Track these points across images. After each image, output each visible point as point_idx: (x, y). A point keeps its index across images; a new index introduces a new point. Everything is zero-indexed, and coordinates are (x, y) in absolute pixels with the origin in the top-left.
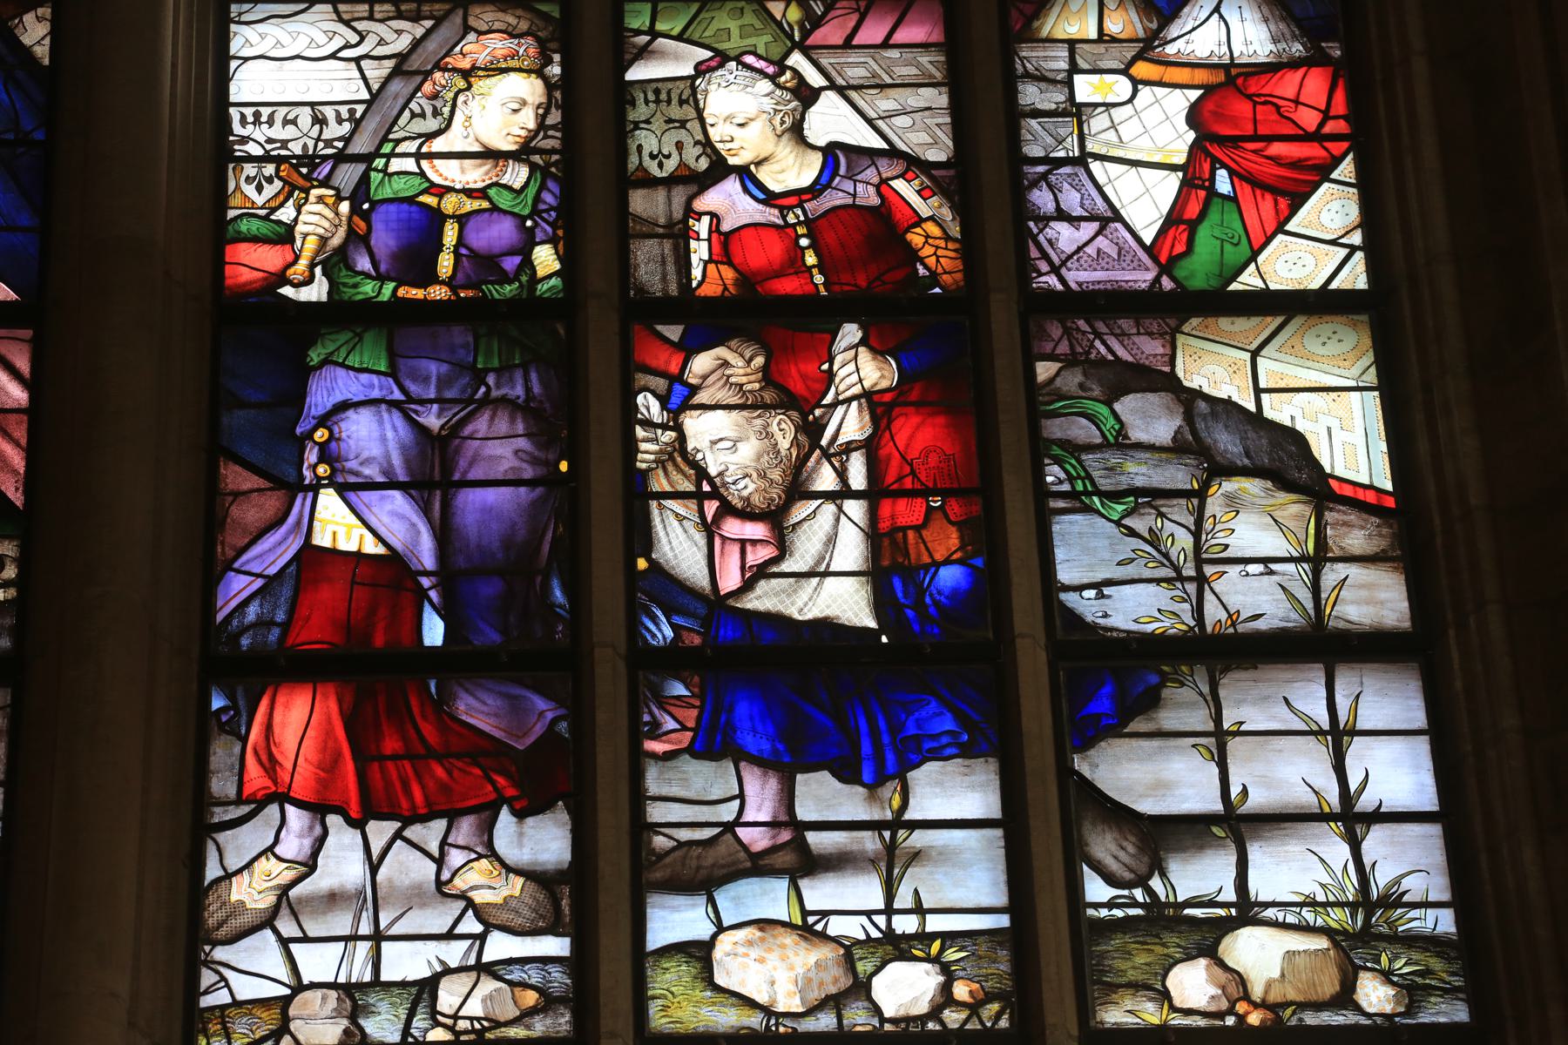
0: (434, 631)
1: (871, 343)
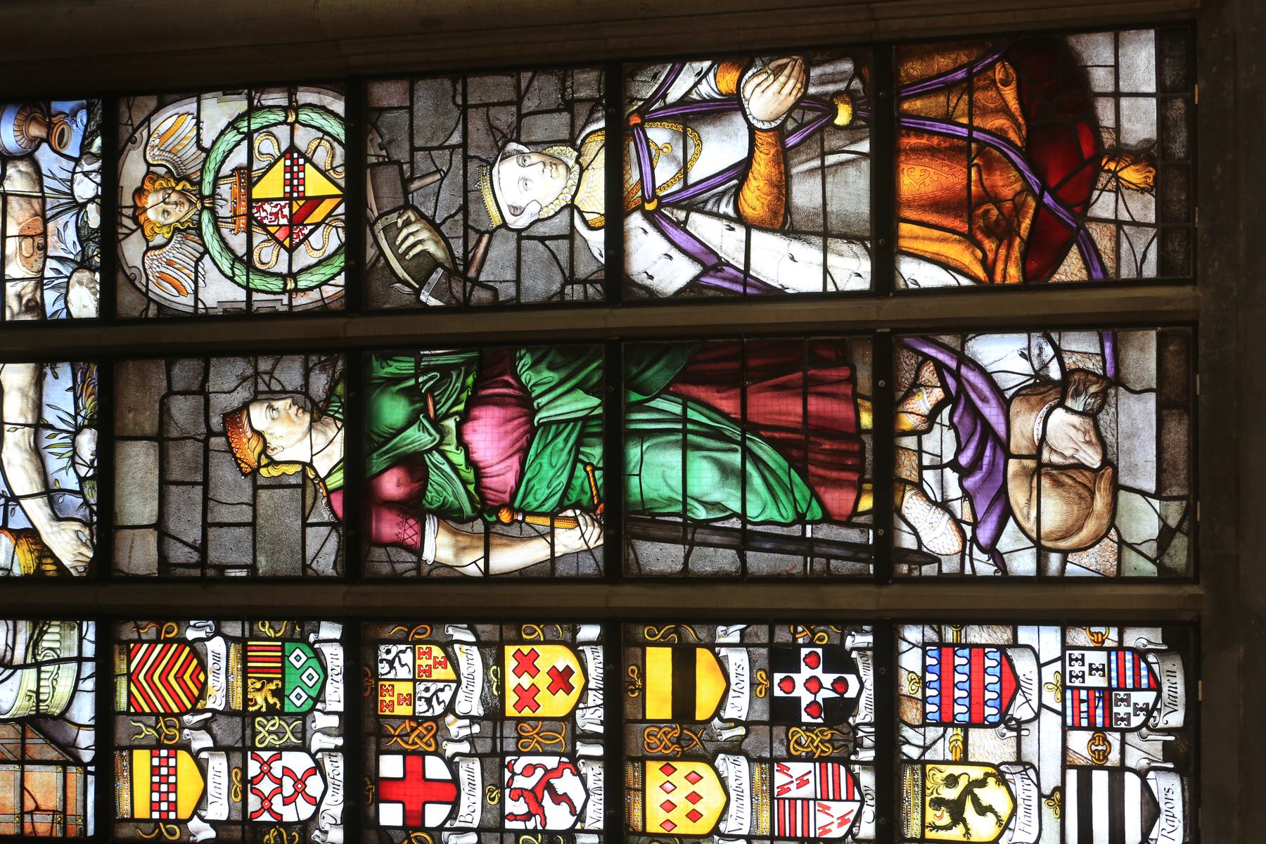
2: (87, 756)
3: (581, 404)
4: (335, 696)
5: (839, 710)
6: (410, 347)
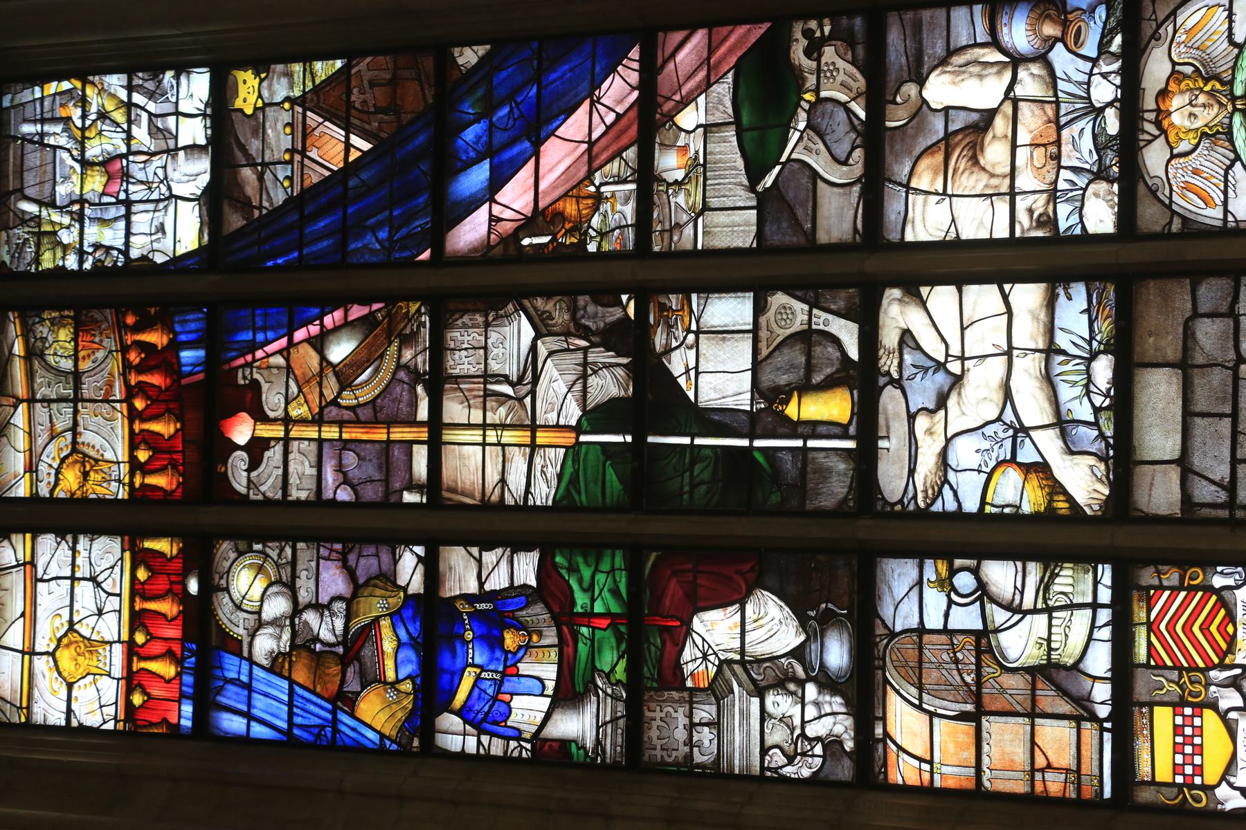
2: (1103, 711)
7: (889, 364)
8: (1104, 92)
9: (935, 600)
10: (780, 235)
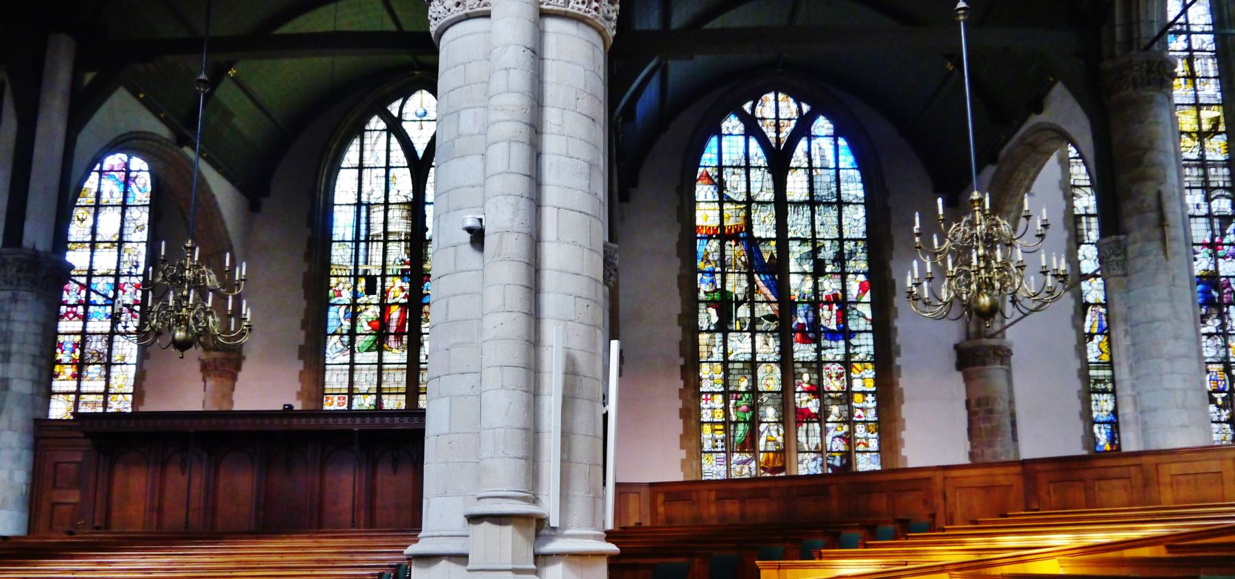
0: (807, 329)
1: (837, 305)
3: (748, 419)
4: (716, 390)
5: (717, 447)
6: (754, 398)
7: (743, 334)
8: (771, 359)
9: (719, 340)
10: (757, 320)
